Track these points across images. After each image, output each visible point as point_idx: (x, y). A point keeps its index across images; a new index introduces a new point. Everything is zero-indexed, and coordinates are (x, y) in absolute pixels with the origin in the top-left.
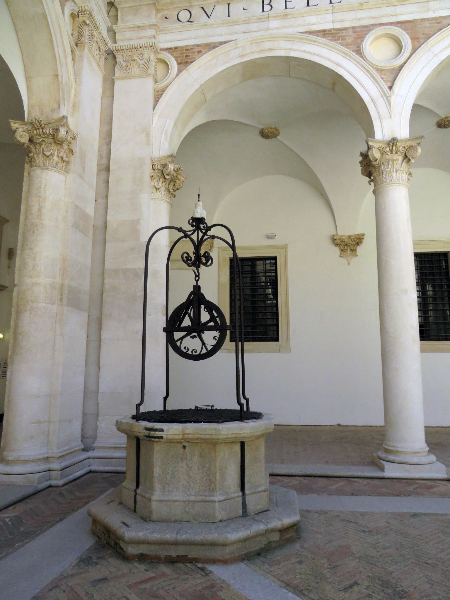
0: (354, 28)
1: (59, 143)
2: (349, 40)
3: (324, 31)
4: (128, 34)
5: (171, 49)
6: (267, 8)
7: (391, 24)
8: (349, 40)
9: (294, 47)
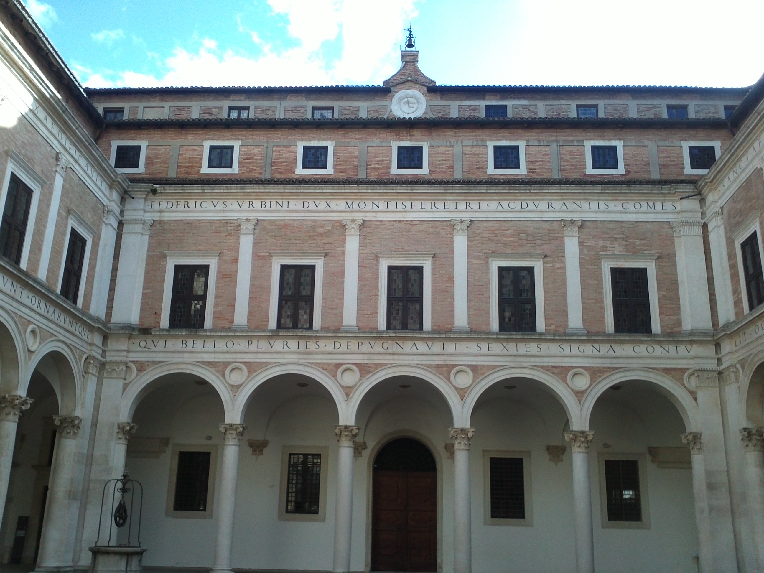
0: (223, 362)
1: (73, 426)
2: (220, 368)
3: (209, 362)
4: (113, 353)
6: (184, 346)
7: (240, 362)
8: (220, 368)
9: (194, 369)
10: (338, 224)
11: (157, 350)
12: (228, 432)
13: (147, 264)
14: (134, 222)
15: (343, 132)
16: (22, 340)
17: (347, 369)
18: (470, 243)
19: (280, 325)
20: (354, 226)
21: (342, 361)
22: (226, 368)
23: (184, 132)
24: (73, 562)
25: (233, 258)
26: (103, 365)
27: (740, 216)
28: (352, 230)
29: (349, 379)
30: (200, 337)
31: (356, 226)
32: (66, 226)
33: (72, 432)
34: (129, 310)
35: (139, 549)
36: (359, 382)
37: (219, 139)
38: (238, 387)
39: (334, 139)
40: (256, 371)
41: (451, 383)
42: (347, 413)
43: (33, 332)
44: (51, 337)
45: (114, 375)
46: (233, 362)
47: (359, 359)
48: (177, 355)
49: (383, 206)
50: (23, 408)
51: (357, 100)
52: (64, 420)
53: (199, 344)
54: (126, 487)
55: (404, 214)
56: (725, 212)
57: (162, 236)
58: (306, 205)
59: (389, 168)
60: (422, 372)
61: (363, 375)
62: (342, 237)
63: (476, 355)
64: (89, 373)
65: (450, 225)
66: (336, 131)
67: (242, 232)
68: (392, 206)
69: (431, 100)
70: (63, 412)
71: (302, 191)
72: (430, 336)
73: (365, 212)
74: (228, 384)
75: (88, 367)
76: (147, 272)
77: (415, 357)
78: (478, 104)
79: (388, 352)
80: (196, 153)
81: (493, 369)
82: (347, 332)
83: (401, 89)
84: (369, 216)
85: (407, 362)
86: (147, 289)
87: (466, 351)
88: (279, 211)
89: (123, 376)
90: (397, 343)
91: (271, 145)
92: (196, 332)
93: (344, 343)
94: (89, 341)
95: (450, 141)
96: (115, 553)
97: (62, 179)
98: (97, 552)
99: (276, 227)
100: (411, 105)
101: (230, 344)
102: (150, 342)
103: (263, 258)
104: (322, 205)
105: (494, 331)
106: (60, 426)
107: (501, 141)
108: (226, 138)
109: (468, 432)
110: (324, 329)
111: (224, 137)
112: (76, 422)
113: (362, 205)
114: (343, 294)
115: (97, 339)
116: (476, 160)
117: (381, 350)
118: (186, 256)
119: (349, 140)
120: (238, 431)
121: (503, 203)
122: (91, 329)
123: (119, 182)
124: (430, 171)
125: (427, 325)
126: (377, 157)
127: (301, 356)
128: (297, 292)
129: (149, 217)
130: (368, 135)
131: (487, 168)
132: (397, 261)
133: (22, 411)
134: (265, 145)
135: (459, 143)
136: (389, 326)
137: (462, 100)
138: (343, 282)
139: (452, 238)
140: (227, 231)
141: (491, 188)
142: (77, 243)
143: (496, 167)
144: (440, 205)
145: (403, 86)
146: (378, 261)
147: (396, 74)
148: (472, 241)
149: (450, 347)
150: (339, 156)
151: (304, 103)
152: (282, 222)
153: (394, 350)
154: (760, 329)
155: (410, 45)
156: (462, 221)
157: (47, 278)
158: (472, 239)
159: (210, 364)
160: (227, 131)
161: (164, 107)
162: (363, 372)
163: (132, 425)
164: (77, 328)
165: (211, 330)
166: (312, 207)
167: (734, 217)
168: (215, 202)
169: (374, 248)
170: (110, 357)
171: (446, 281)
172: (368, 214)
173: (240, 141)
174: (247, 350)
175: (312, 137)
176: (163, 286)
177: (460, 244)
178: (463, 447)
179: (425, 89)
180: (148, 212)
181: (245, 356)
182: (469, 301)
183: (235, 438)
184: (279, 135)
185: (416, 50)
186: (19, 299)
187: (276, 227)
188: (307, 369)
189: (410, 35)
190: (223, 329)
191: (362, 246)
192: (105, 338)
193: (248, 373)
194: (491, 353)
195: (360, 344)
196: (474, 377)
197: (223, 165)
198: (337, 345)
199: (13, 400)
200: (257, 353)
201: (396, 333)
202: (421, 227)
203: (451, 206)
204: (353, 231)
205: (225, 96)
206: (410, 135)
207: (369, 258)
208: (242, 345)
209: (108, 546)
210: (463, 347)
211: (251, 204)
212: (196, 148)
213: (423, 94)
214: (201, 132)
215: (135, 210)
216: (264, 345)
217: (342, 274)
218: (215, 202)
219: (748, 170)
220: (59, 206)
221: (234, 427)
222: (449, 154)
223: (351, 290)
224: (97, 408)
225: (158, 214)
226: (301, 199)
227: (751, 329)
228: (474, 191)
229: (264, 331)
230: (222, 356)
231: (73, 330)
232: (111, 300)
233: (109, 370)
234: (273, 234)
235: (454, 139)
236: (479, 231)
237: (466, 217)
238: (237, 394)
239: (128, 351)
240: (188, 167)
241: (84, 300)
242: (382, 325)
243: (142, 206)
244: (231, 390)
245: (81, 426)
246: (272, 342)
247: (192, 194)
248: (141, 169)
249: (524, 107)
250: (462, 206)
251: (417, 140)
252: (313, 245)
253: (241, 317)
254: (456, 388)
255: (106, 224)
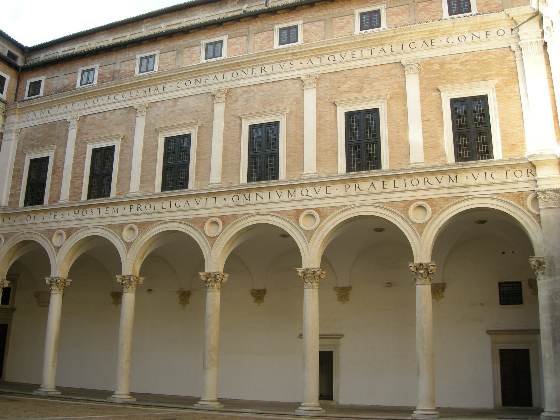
27: (37, 142)
56: (23, 133)
154: (32, 218)
167: (31, 140)
219: (57, 117)
227: (24, 216)
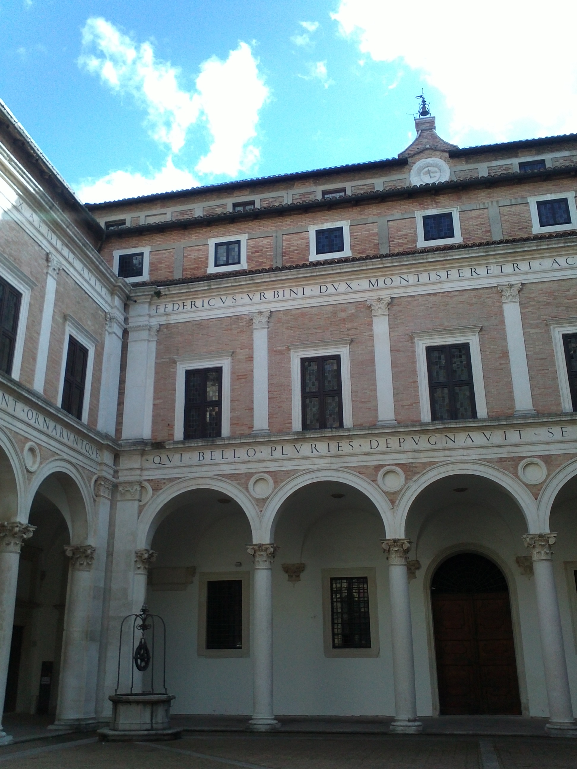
0: (245, 473)
1: (87, 557)
3: (230, 474)
4: (125, 473)
5: (149, 480)
6: (201, 458)
7: (264, 472)
8: (243, 481)
10: (362, 306)
11: (172, 466)
12: (257, 554)
13: (156, 373)
14: (139, 328)
15: (359, 209)
16: (19, 460)
17: (390, 472)
18: (523, 311)
19: (305, 426)
20: (381, 306)
21: (381, 463)
22: (249, 479)
23: (187, 232)
24: (96, 713)
25: (247, 356)
26: (115, 487)
28: (380, 310)
29: (393, 483)
30: (218, 447)
31: (383, 306)
32: (63, 333)
33: (85, 563)
34: (140, 424)
35: (164, 697)
36: (405, 486)
37: (224, 235)
38: (264, 500)
39: (349, 219)
40: (282, 481)
41: (520, 479)
42: (395, 524)
43: (31, 450)
44: (53, 456)
45: (128, 496)
46: (256, 473)
47: (401, 458)
48: (194, 469)
49: (412, 279)
50: (25, 536)
51: (371, 178)
52: (76, 550)
53: (217, 454)
54: (147, 623)
55: (439, 286)
57: (169, 340)
58: (324, 289)
59: (415, 241)
60: (482, 468)
61: (409, 477)
62: (368, 319)
63: (548, 443)
64: (100, 496)
65: (498, 291)
66: (350, 210)
67: (255, 327)
68: (424, 278)
69: (455, 166)
70: (75, 541)
71: (318, 274)
72: (487, 424)
73: (392, 288)
74: (253, 497)
75: (99, 489)
76: (157, 382)
77: (471, 451)
78: (510, 163)
79: (437, 448)
80: (201, 253)
81: (571, 458)
82: (384, 427)
83: (419, 159)
84: (398, 293)
85: (462, 457)
86: (158, 399)
87: (534, 439)
88: (294, 299)
89: (137, 497)
90: (446, 436)
91: (280, 233)
92: (213, 441)
93: (382, 441)
94: (99, 460)
95: (484, 203)
96: (138, 703)
97: (55, 283)
98: (117, 701)
99: (292, 317)
100: (432, 175)
101: (251, 452)
102: (164, 457)
103: (280, 353)
104: (342, 287)
105: (568, 411)
106: (72, 557)
107: (545, 196)
108: (231, 234)
109: (548, 538)
110: (357, 426)
111: (229, 232)
112: (89, 552)
113: (388, 281)
114: (375, 384)
115: (107, 458)
116: (518, 220)
117: (429, 446)
118: (196, 359)
119: (367, 217)
120: (269, 552)
121: (558, 259)
122: (100, 447)
123: (120, 287)
124: (463, 239)
125: (482, 411)
126: (400, 231)
127: (333, 460)
128: (322, 386)
129: (155, 322)
130: (387, 209)
131: (532, 227)
132: (436, 341)
133: (24, 541)
134: (274, 235)
135: (495, 203)
136: (435, 416)
137: (491, 161)
138: (374, 371)
139: (501, 307)
140: (238, 328)
141: (543, 243)
142: (77, 354)
143: (542, 225)
144: (481, 271)
145: (421, 155)
146: (413, 343)
147: (411, 145)
148: (527, 308)
149: (513, 436)
150: (357, 235)
151: (313, 188)
152: (299, 311)
153: (444, 444)
155: (424, 112)
156: (511, 286)
157: (45, 390)
158: (526, 305)
159: (231, 476)
160: (232, 225)
161: (166, 214)
162: (409, 473)
163: (151, 552)
164: (83, 446)
165: (229, 438)
166: (331, 290)
168: (224, 298)
169: (407, 328)
170: (123, 477)
171: (500, 357)
172: (396, 291)
173: (247, 234)
174: (271, 457)
175: (323, 219)
176: (174, 395)
177: (512, 312)
178: (543, 557)
179: (447, 155)
180: (154, 316)
181: (268, 464)
182: (531, 378)
183: (266, 561)
184: (288, 222)
185: (432, 116)
186: (12, 412)
187: (292, 317)
188: (341, 474)
189: (424, 101)
190: (242, 436)
191: (392, 327)
192: (117, 457)
193: (274, 484)
194: (566, 438)
195: (402, 440)
196: (548, 470)
197: (230, 262)
198: (374, 444)
199: (13, 527)
200: (283, 460)
201: (444, 424)
202: (462, 299)
203: (495, 269)
204: (380, 312)
205: (228, 194)
206: (436, 203)
207: (401, 340)
208: (264, 452)
209: (131, 694)
210: (530, 435)
211: (262, 296)
212: (200, 247)
213: (445, 161)
214: (204, 230)
215: (139, 316)
216: (289, 449)
217: (372, 361)
218: (224, 298)
220: (54, 311)
221: (264, 547)
222: (483, 218)
223: (384, 378)
224: (111, 535)
225: (164, 318)
226: (317, 283)
228: (522, 250)
229: (288, 434)
230: (244, 466)
231: (79, 448)
232: (120, 414)
233: (123, 491)
234: (290, 325)
235: (488, 200)
236: (533, 295)
237: (515, 280)
238: (264, 509)
239: (142, 469)
240: (194, 269)
241: (90, 415)
242: (426, 415)
243: (146, 312)
244: (257, 505)
245: (95, 556)
246: (298, 446)
247: (199, 292)
248: (145, 277)
249: (565, 158)
250: (508, 268)
251: (445, 207)
252: (336, 332)
253: (261, 420)
254: (526, 485)
255: (109, 333)
